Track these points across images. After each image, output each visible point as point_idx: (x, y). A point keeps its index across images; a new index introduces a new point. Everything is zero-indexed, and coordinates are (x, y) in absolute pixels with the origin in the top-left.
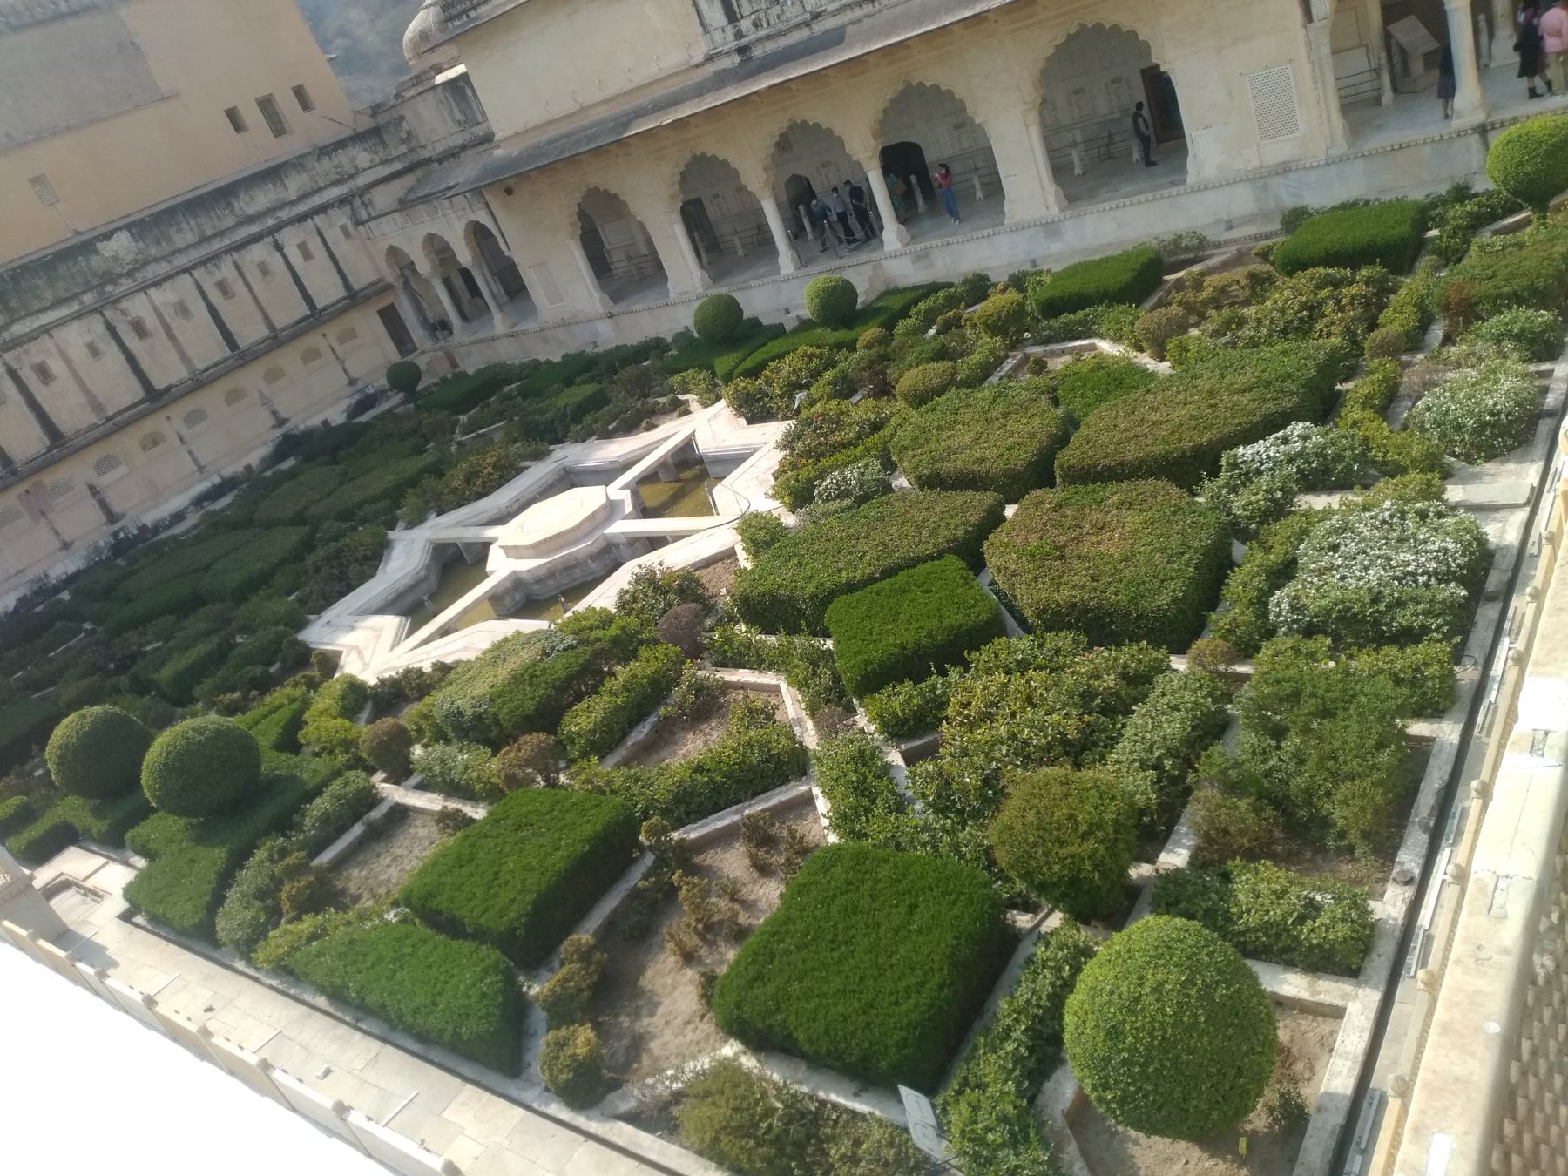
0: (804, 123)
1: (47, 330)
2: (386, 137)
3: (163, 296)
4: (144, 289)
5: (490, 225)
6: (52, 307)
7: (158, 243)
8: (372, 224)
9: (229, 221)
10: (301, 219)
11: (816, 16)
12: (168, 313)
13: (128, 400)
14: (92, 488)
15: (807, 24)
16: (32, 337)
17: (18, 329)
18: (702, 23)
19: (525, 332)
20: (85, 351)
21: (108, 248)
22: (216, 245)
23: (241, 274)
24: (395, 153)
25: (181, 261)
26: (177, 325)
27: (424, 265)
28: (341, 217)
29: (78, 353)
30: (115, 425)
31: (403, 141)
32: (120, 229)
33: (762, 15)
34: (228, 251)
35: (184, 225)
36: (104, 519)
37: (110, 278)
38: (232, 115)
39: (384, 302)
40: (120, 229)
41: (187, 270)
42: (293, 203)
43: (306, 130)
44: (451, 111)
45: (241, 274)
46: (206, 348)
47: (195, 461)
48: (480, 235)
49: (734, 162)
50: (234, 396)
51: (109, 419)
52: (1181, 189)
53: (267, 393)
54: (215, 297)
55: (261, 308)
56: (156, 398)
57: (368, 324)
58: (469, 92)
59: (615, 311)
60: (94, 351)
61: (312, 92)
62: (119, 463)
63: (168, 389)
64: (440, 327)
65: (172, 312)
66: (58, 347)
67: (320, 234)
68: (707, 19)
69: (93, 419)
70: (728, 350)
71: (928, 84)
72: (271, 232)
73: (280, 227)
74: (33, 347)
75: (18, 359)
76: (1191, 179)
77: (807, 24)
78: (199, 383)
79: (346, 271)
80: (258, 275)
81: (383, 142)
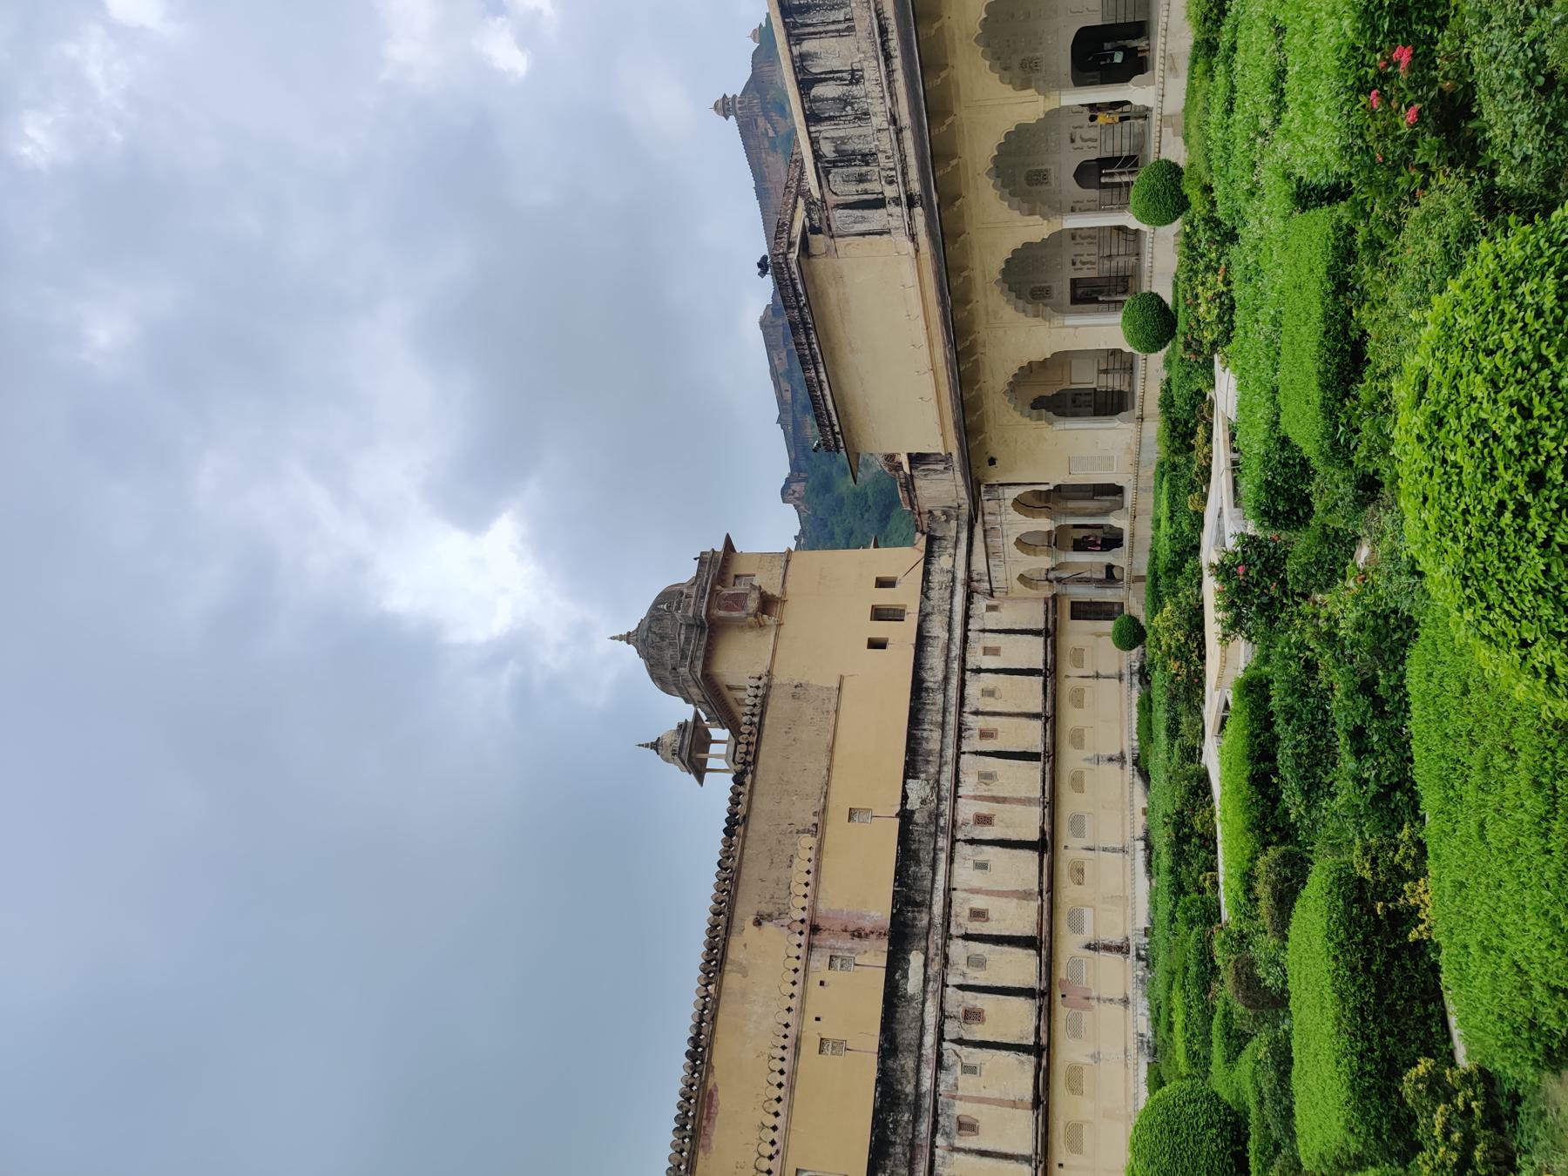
1: (949, 890)
3: (968, 786)
4: (956, 797)
6: (934, 874)
7: (928, 762)
9: (939, 698)
10: (965, 639)
11: (894, 120)
14: (1088, 947)
15: (899, 131)
16: (948, 904)
17: (938, 908)
18: (880, 233)
19: (1135, 504)
20: (978, 872)
21: (914, 803)
22: (952, 719)
24: (953, 534)
25: (950, 753)
26: (996, 789)
28: (980, 604)
30: (1049, 889)
31: (947, 521)
33: (883, 173)
34: (960, 713)
35: (925, 734)
36: (1120, 956)
37: (936, 815)
38: (877, 644)
40: (904, 783)
41: (959, 753)
42: (950, 639)
43: (906, 595)
46: (1027, 779)
47: (1114, 850)
51: (1041, 893)
56: (1045, 846)
59: (1137, 412)
60: (982, 866)
61: (886, 574)
62: (1081, 913)
63: (1042, 831)
64: (1110, 576)
67: (984, 631)
69: (1035, 904)
71: (984, 15)
72: (963, 670)
73: (963, 660)
74: (955, 908)
75: (959, 925)
77: (899, 131)
78: (1051, 804)
79: (1024, 627)
80: (990, 700)
81: (940, 538)
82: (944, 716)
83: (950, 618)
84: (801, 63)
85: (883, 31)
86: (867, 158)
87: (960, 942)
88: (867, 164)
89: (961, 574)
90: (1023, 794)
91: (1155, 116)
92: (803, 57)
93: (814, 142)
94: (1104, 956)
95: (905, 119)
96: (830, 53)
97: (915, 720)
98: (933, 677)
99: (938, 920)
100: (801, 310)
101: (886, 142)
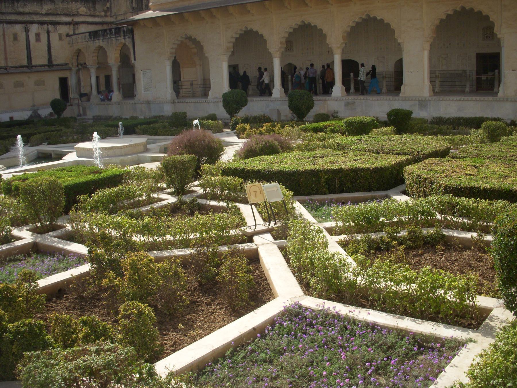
8: (74, 37)
9: (10, 10)
10: (41, 23)
24: (98, 14)
39: (62, 74)
49: (266, 35)
52: (495, 98)
55: (6, 54)
57: (52, 82)
59: (176, 101)
67: (48, 32)
71: (378, 18)
73: (32, 22)
76: (500, 94)
80: (12, 39)
81: (94, 7)
83: (53, 15)
89: (77, 19)
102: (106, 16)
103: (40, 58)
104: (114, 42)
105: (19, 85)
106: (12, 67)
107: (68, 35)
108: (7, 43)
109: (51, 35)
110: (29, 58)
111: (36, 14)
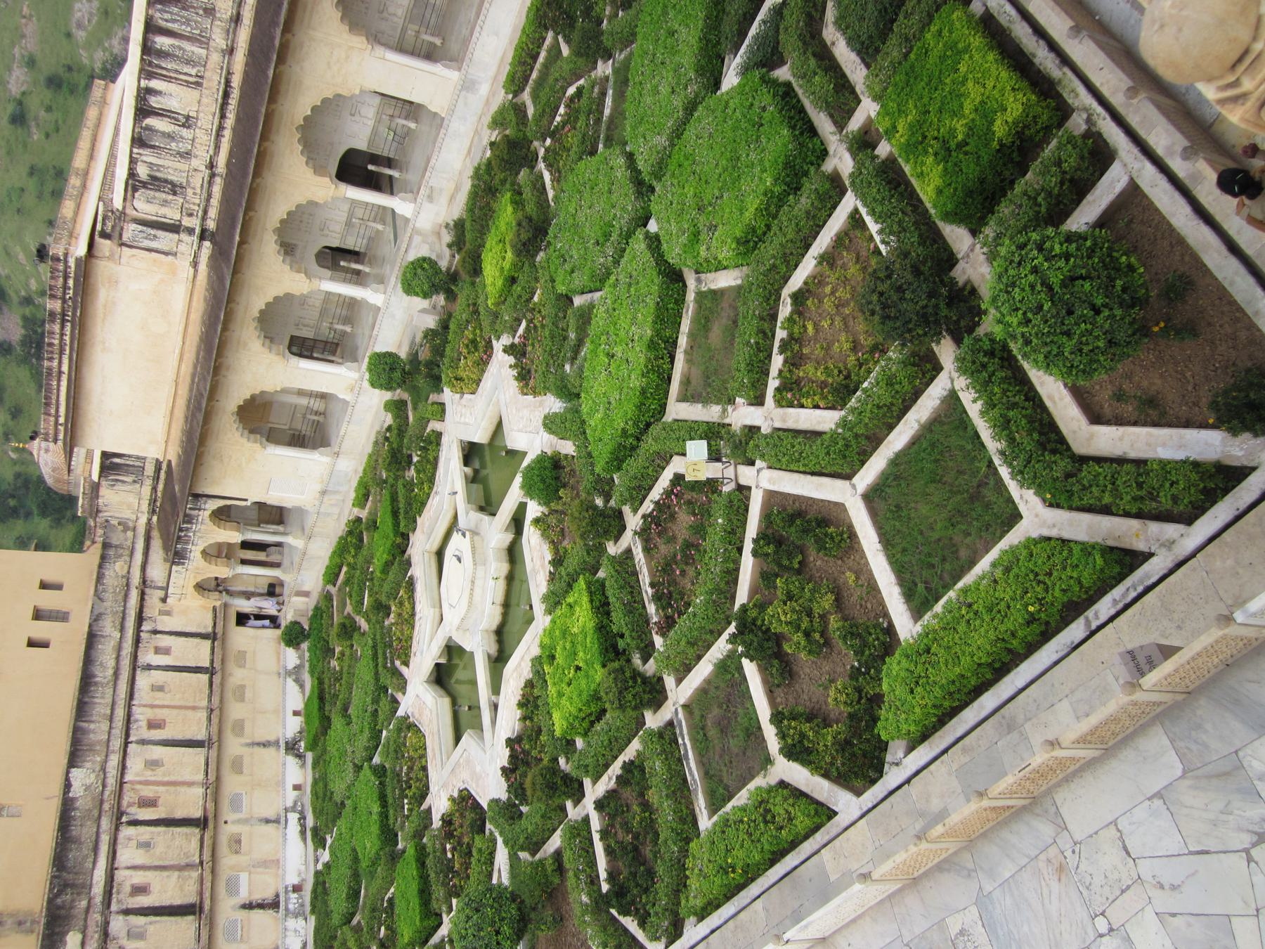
0: (282, 221)
2: (115, 541)
5: (222, 503)
9: (109, 691)
10: (137, 641)
11: (211, 166)
12: (149, 775)
13: (194, 844)
15: (213, 176)
17: (98, 889)
18: (166, 254)
20: (141, 851)
21: (77, 790)
22: (120, 712)
23: (152, 706)
24: (129, 543)
25: (117, 744)
26: (159, 775)
27: (222, 571)
29: (140, 857)
32: (68, 773)
40: (68, 773)
44: (123, 482)
45: (152, 706)
48: (224, 515)
50: (238, 766)
53: (248, 741)
54: (157, 734)
57: (242, 637)
58: (117, 460)
59: (336, 450)
60: (146, 845)
61: (50, 577)
62: (238, 878)
65: (150, 773)
66: (128, 868)
67: (155, 632)
68: (166, 249)
70: (415, 377)
71: (309, 113)
73: (135, 657)
77: (213, 176)
78: (214, 788)
80: (160, 694)
81: (116, 547)
82: (113, 710)
83: (124, 618)
84: (144, 94)
85: (226, 95)
86: (175, 188)
87: (121, 917)
88: (175, 194)
89: (136, 579)
90: (188, 778)
91: (411, 225)
92: (149, 91)
93: (133, 161)
94: (257, 914)
95: (221, 167)
96: (174, 97)
97: (82, 709)
98: (103, 673)
99: (98, 900)
100: (64, 301)
101: (197, 181)
102: (134, 529)
103: (200, 653)
104: (203, 527)
105: (240, 693)
106: (210, 700)
107: (164, 600)
108: (166, 703)
109: (159, 628)
110: (197, 670)
111: (119, 648)
